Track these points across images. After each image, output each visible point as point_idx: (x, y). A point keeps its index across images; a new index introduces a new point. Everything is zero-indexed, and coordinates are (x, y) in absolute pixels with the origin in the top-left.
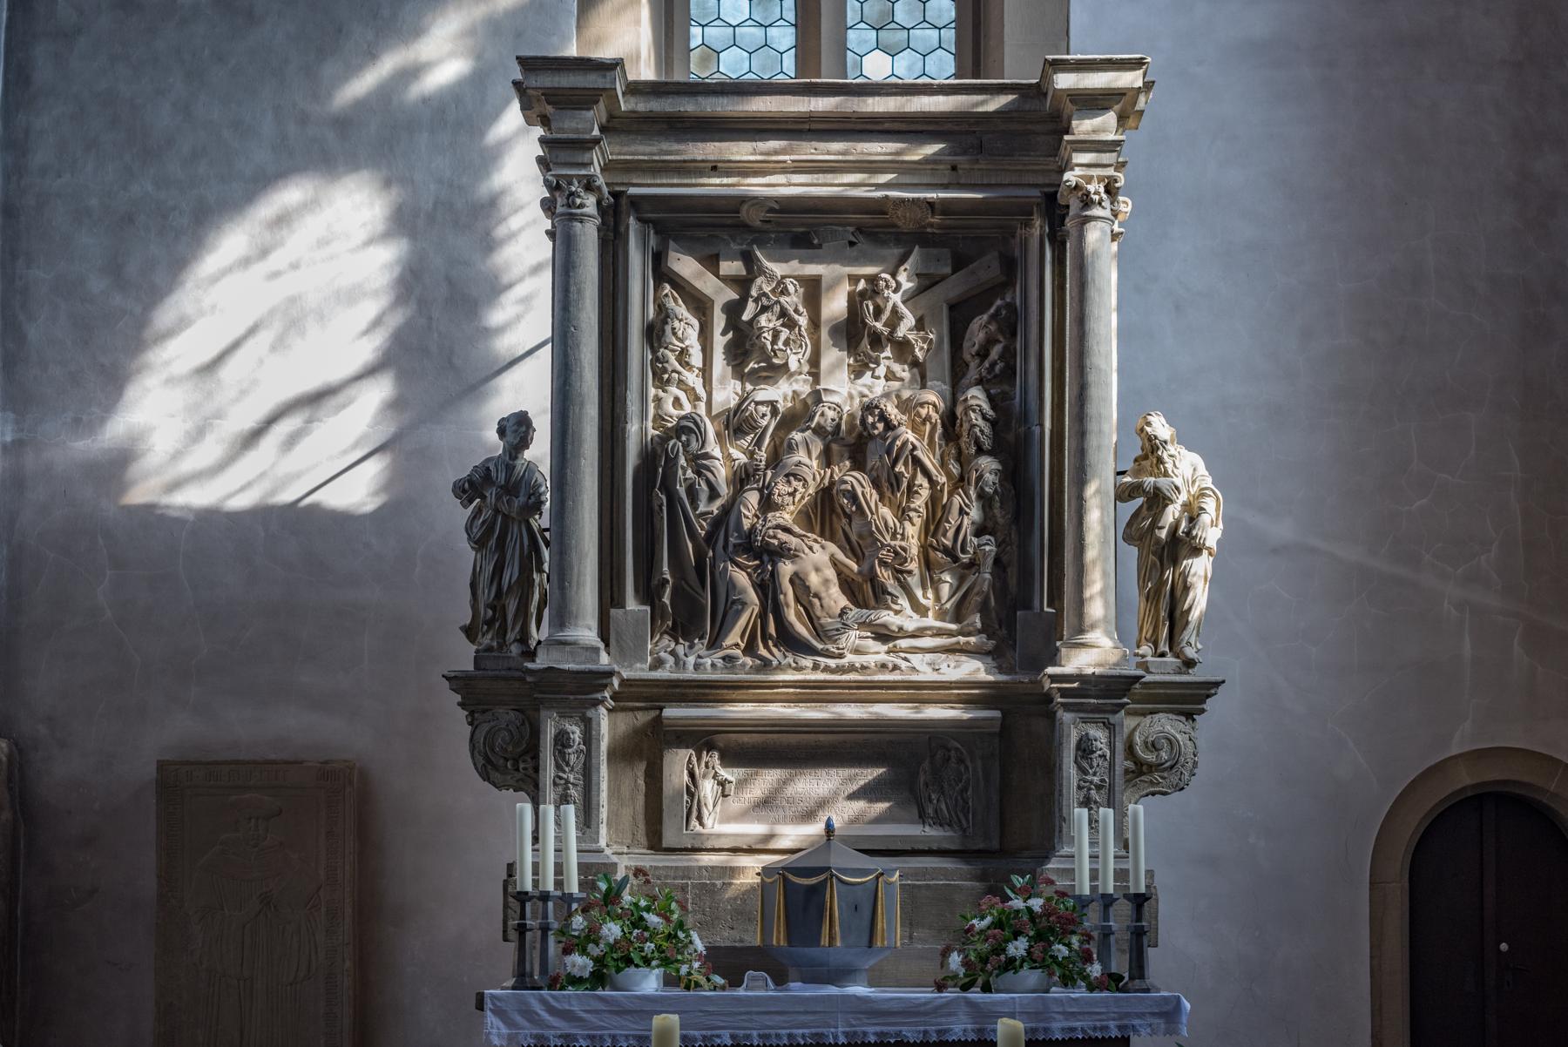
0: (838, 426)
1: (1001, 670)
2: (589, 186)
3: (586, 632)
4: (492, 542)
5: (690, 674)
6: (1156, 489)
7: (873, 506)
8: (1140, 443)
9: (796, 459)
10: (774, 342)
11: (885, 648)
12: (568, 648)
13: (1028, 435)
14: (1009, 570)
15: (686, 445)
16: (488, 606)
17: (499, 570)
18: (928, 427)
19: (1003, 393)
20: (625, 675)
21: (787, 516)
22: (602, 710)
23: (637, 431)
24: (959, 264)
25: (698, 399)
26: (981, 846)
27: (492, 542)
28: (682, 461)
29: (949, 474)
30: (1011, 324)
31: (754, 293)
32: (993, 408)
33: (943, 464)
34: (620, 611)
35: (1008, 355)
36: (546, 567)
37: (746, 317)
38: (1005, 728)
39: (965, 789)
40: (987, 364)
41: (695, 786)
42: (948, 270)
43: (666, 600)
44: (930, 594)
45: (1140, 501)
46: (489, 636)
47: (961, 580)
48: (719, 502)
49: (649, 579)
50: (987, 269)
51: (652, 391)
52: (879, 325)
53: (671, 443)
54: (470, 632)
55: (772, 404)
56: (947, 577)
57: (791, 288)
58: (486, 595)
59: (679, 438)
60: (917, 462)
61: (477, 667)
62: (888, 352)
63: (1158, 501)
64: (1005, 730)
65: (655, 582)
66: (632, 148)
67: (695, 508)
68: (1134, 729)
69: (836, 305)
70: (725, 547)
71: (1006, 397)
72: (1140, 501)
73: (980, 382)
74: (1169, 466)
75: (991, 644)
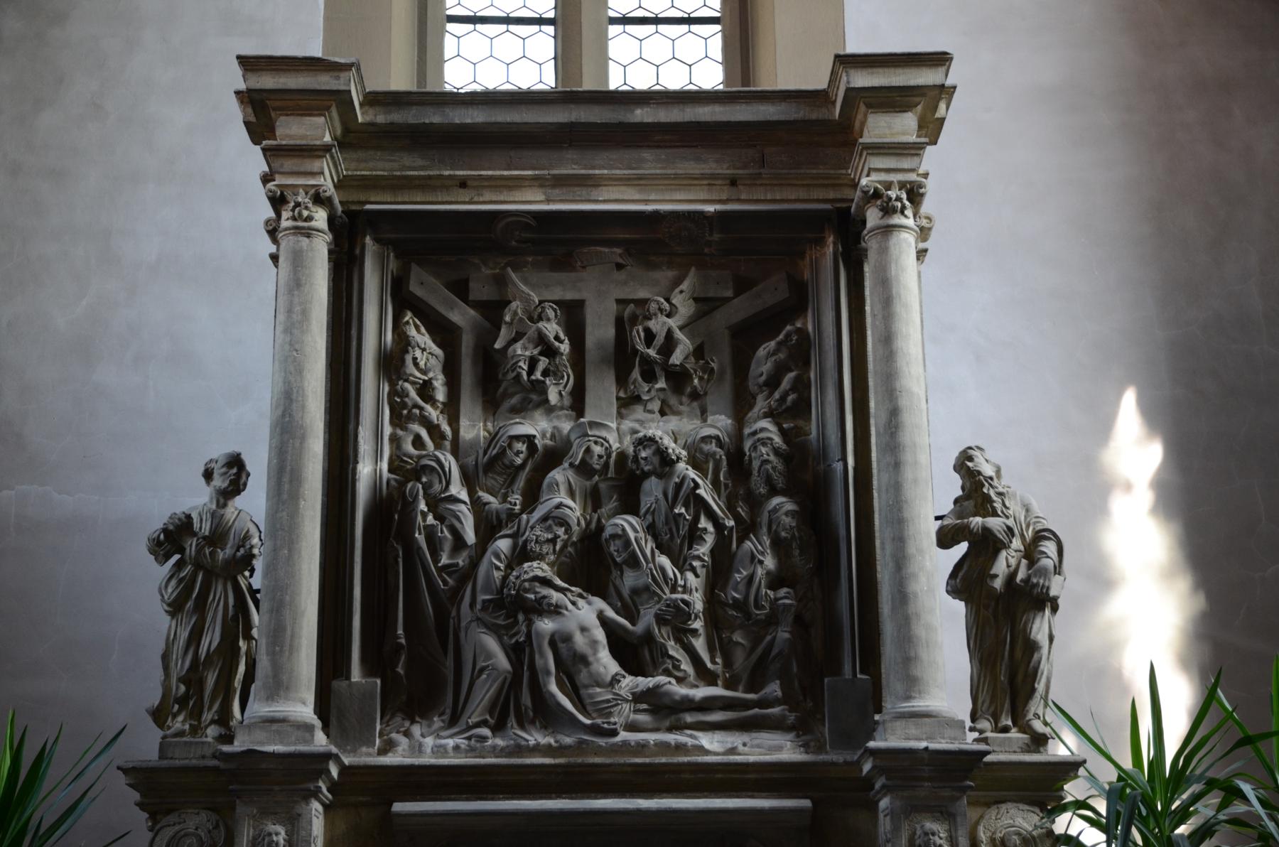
0: (606, 465)
1: (806, 747)
2: (319, 199)
4: (190, 604)
5: (427, 760)
6: (987, 531)
8: (960, 482)
9: (557, 501)
10: (531, 371)
11: (667, 723)
12: (275, 727)
13: (829, 472)
15: (427, 487)
16: (180, 680)
17: (196, 636)
19: (796, 427)
20: (347, 760)
21: (545, 567)
22: (316, 806)
24: (742, 286)
25: (443, 436)
27: (190, 604)
28: (423, 506)
29: (737, 517)
30: (801, 353)
31: (507, 318)
33: (731, 508)
34: (344, 684)
35: (801, 386)
36: (255, 632)
37: (497, 346)
40: (777, 395)
42: (729, 293)
43: (400, 670)
44: (719, 660)
45: (962, 548)
46: (180, 718)
47: (756, 641)
48: (465, 554)
50: (773, 292)
51: (388, 430)
52: (652, 352)
53: (410, 485)
54: (159, 715)
55: (529, 439)
56: (738, 637)
57: (551, 313)
58: (181, 666)
59: (419, 480)
61: (162, 756)
62: (661, 384)
63: (986, 546)
66: (371, 164)
67: (436, 561)
68: (977, 823)
69: (600, 331)
72: (962, 548)
73: (770, 414)
74: (998, 506)
75: (792, 718)
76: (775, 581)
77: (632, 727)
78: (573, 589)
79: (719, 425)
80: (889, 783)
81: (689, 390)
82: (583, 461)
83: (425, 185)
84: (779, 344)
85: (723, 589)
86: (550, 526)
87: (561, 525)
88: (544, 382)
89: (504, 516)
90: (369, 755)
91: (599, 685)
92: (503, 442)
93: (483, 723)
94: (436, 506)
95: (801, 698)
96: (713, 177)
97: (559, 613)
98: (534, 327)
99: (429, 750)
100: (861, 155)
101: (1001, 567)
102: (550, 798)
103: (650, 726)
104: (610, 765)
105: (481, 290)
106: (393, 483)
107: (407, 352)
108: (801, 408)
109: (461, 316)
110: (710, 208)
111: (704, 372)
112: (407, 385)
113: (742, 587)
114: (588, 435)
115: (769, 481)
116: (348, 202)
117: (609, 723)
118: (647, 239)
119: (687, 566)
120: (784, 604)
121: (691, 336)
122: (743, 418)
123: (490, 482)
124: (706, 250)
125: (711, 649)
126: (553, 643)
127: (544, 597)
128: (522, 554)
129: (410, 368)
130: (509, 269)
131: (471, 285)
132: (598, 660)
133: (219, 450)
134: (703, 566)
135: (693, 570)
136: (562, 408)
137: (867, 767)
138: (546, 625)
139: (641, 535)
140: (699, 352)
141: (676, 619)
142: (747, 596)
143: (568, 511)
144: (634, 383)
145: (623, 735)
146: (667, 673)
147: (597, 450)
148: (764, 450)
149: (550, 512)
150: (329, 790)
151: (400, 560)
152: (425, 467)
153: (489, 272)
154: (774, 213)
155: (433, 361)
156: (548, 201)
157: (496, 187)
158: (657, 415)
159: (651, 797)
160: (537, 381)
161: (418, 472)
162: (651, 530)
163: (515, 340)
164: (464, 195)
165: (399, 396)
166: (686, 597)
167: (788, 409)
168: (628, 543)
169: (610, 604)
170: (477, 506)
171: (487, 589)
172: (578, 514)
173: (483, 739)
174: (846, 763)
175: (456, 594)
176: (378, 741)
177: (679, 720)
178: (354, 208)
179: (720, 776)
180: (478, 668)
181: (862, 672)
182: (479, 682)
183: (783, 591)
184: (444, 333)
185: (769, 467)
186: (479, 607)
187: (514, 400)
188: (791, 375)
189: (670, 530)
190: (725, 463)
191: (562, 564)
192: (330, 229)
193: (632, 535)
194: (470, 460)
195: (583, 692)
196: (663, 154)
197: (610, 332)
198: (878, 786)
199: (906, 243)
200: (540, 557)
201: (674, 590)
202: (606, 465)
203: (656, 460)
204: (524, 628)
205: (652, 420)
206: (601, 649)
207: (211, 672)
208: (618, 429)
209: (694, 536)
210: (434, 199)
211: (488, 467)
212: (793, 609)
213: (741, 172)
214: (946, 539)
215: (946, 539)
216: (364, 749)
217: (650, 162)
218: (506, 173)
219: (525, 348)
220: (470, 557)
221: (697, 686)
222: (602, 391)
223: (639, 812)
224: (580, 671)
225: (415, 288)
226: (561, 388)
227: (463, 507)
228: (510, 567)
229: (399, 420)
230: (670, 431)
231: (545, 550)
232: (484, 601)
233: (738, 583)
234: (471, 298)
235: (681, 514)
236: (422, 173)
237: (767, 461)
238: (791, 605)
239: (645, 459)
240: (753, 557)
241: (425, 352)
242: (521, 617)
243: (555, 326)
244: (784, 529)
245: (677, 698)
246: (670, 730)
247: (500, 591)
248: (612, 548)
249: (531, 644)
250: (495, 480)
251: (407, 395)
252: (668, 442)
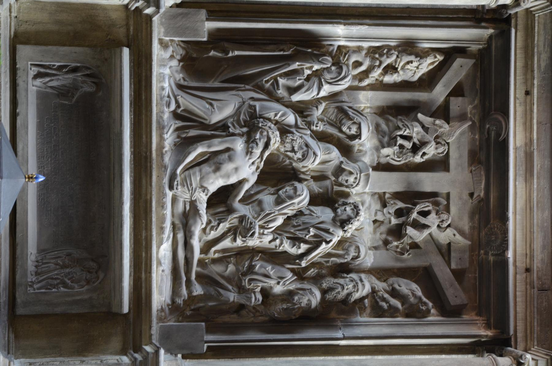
0: (341, 185)
5: (156, 70)
7: (285, 211)
9: (319, 153)
10: (403, 137)
11: (177, 222)
14: (235, 316)
18: (341, 252)
19: (365, 308)
20: (155, 19)
21: (276, 145)
24: (458, 275)
25: (361, 80)
26: (19, 300)
28: (316, 67)
29: (307, 269)
30: (414, 312)
31: (438, 122)
32: (356, 302)
33: (313, 265)
35: (392, 312)
37: (420, 116)
39: (65, 286)
40: (386, 296)
41: (67, 73)
42: (453, 266)
43: (212, 53)
44: (217, 255)
47: (228, 279)
49: (228, 41)
50: (454, 294)
52: (414, 215)
53: (329, 59)
55: (358, 136)
56: (231, 268)
59: (333, 64)
60: (317, 245)
62: (394, 221)
64: (111, 316)
65: (226, 45)
66: (542, 32)
67: (281, 76)
69: (428, 182)
70: (252, 99)
71: (363, 309)
73: (374, 291)
76: (266, 293)
77: (174, 200)
78: (262, 163)
79: (367, 258)
80: (138, 362)
81: (390, 238)
82: (343, 170)
83: (528, 68)
84: (420, 298)
85: (261, 259)
86: (302, 149)
87: (303, 156)
88: (395, 145)
89: (309, 119)
90: (159, 33)
91: (201, 179)
92: (357, 119)
93: (178, 106)
94: (316, 76)
95: (192, 308)
96: (532, 257)
97: (247, 154)
98: (432, 139)
99: (161, 71)
100: (547, 355)
102: (131, 148)
103: (175, 211)
104: (151, 185)
105: (456, 104)
106: (331, 48)
107: (416, 57)
108: (378, 311)
109: (439, 93)
110: (510, 254)
111: (401, 249)
112: (394, 57)
113: (262, 271)
114: (361, 173)
115: (331, 289)
116: (517, 18)
117: (177, 185)
119: (276, 236)
120: (251, 298)
121: (425, 241)
122: (371, 273)
123: (331, 110)
124: (482, 252)
125: (224, 251)
126: (228, 150)
127: (257, 144)
128: (285, 131)
129: (406, 59)
130: (470, 123)
131: (460, 99)
132: (217, 178)
134: (276, 246)
135: (274, 240)
136: (378, 157)
137: (148, 349)
138: (239, 145)
139: (296, 207)
140: (415, 246)
141: (243, 229)
142: (257, 274)
143: (312, 160)
144: (395, 203)
145: (170, 194)
146: (209, 222)
147: (351, 179)
148: (351, 286)
149: (312, 149)
150: (137, 8)
151: (281, 53)
152: (341, 68)
153: (469, 110)
155: (410, 74)
156: (516, 149)
157: (526, 114)
158: (374, 218)
159: (131, 211)
160: (396, 141)
161: (337, 64)
162: (300, 213)
163: (423, 127)
164: (521, 94)
165: (387, 52)
166: (257, 235)
167: (377, 302)
168: (291, 198)
169: (253, 186)
170: (316, 102)
171: (263, 108)
172: (310, 166)
173: (168, 105)
174: (151, 335)
175: (260, 88)
176: (168, 39)
177: (179, 229)
178: (513, 21)
179: (144, 255)
180: (213, 102)
181: (208, 347)
182: (204, 102)
183: (260, 297)
184: (429, 81)
185: (340, 289)
186: (252, 103)
187: (384, 127)
188: (399, 304)
189: (299, 226)
190: (342, 261)
191: (279, 156)
192: (499, 6)
193: (296, 201)
194: (345, 98)
195: (197, 169)
196: (547, 224)
197: (428, 188)
198: (136, 355)
200: (283, 142)
201: (261, 227)
202: (341, 185)
203: (344, 217)
204: (237, 131)
205: (370, 215)
206: (224, 180)
208: (365, 193)
209: (296, 240)
210: (517, 74)
212: (248, 303)
213: (535, 275)
216: (163, 30)
218: (535, 121)
219: (418, 133)
220: (283, 98)
221: (200, 241)
223: (121, 203)
224: (210, 167)
225: (459, 61)
226: (392, 156)
227: (315, 93)
228: (277, 123)
229: (374, 52)
231: (287, 145)
232: (255, 106)
233: (265, 268)
234: (452, 99)
235: (309, 232)
236: (536, 66)
237: (343, 288)
238: (251, 302)
239: (345, 210)
240: (282, 278)
241: (416, 69)
242: (245, 130)
243: (432, 153)
244: (299, 299)
245: (193, 229)
246: (173, 224)
247: (261, 117)
248: (288, 188)
249: (227, 136)
250: (332, 114)
251: (388, 57)
252: (356, 224)
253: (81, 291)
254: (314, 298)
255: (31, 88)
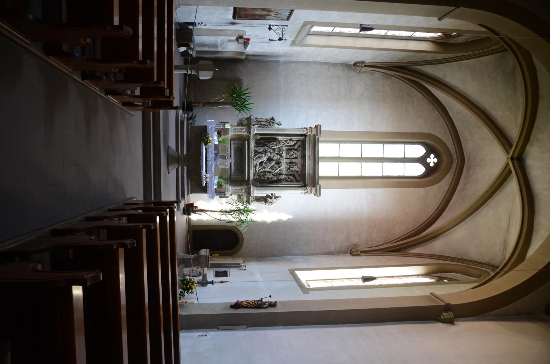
3: (255, 132)
23: (280, 138)
24: (299, 175)
30: (292, 181)
35: (288, 181)
38: (244, 180)
50: (298, 178)
54: (256, 118)
58: (260, 120)
63: (271, 198)
69: (294, 161)
76: (268, 178)
101: (269, 199)
105: (299, 149)
118: (304, 166)
128: (271, 153)
133: (282, 123)
141: (264, 168)
154: (304, 179)
199: (302, 192)
207: (259, 123)
209: (272, 170)
211: (280, 149)
214: (272, 194)
215: (272, 194)
217: (312, 166)
222: (288, 161)
230: (284, 167)
253: (240, 177)
254: (276, 178)
255: (233, 147)
